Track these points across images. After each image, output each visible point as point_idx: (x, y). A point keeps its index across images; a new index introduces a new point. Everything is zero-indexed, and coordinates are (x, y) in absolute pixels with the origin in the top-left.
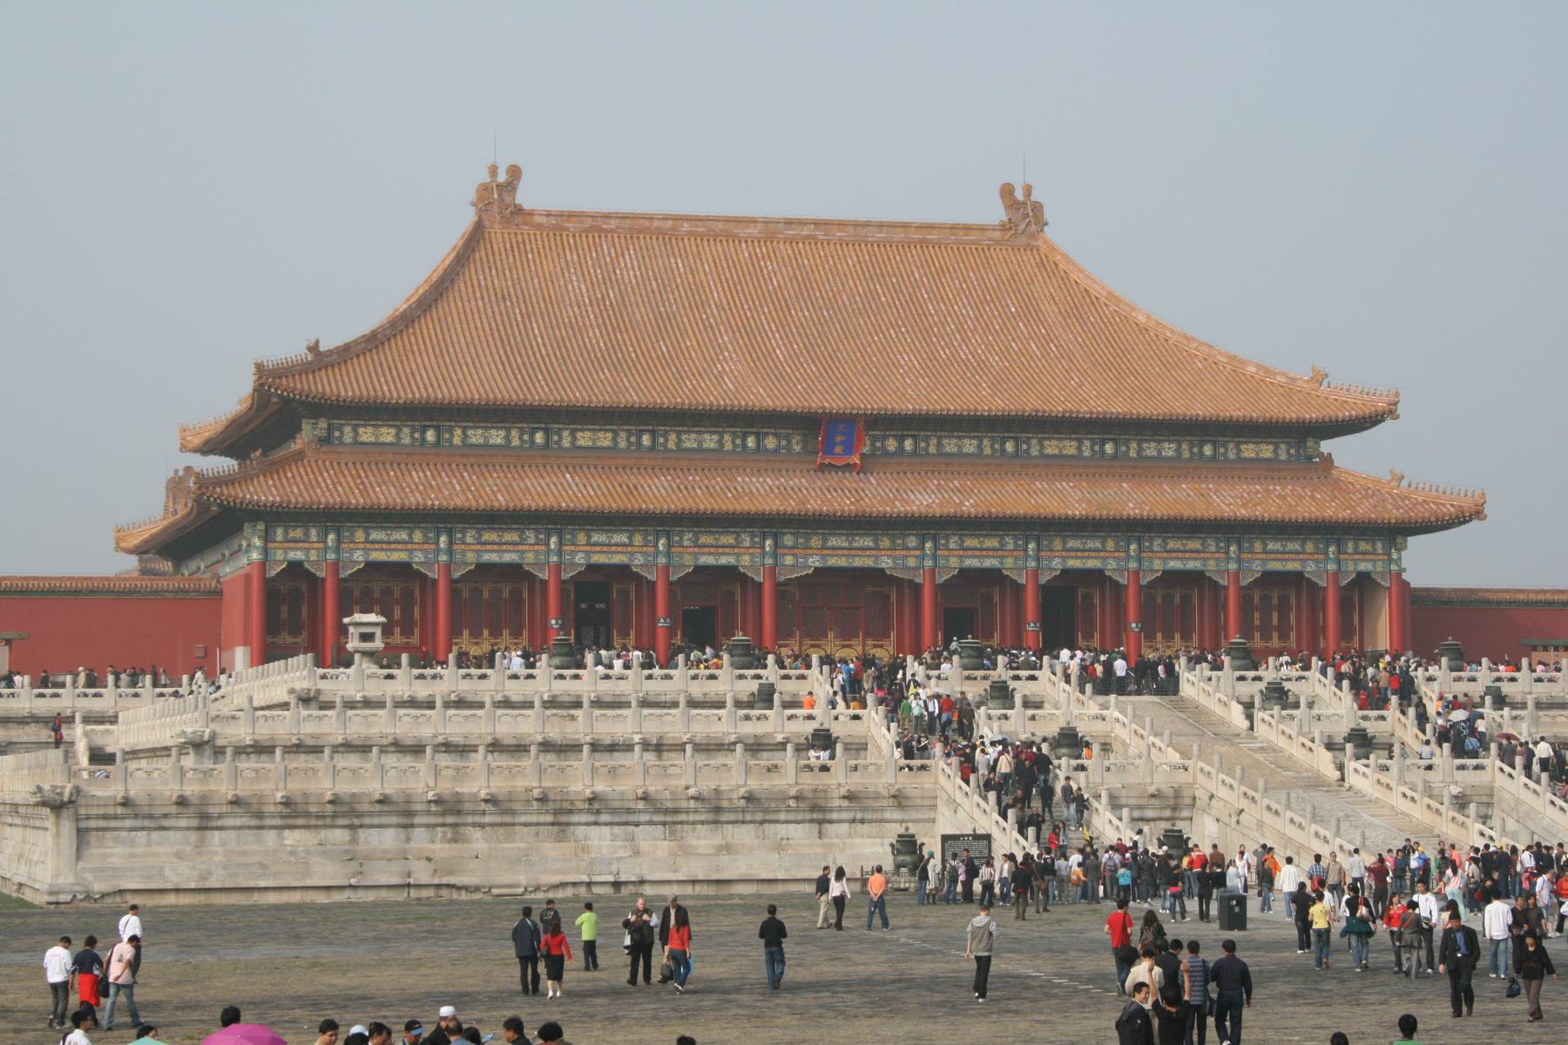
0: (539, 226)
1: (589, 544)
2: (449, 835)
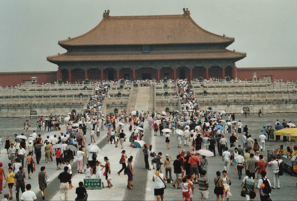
2: (14, 110)
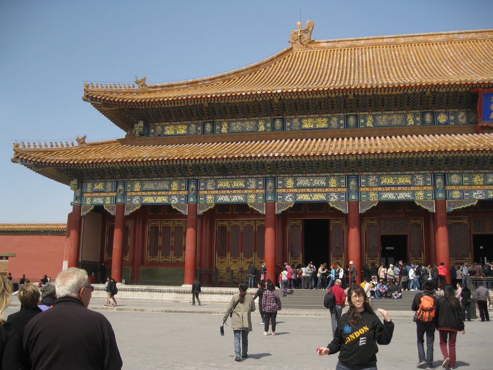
0: (322, 47)
1: (295, 187)
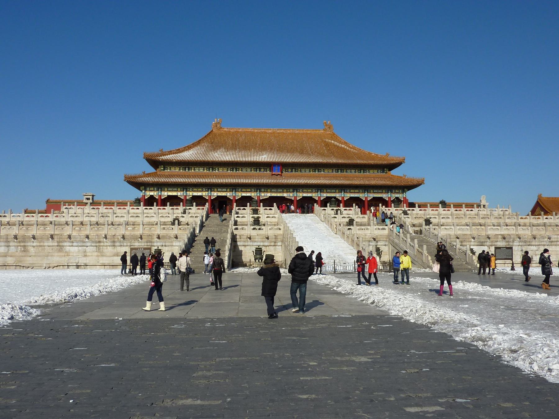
2: (22, 249)
